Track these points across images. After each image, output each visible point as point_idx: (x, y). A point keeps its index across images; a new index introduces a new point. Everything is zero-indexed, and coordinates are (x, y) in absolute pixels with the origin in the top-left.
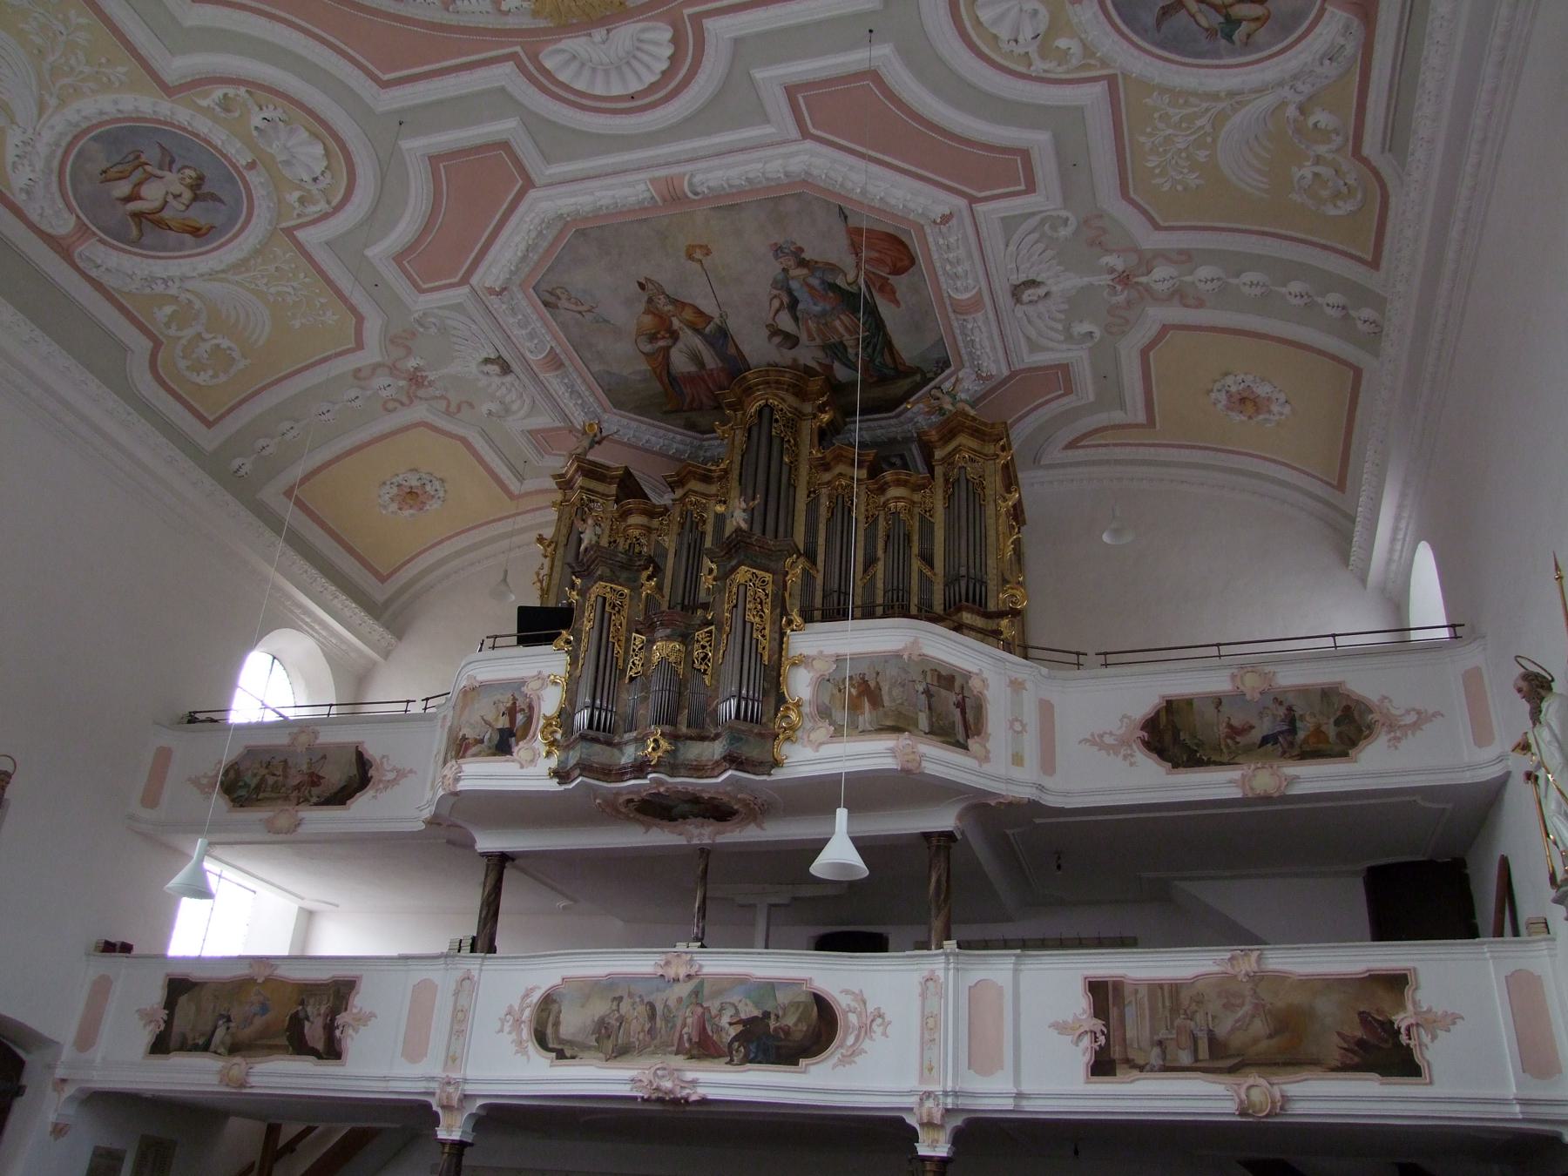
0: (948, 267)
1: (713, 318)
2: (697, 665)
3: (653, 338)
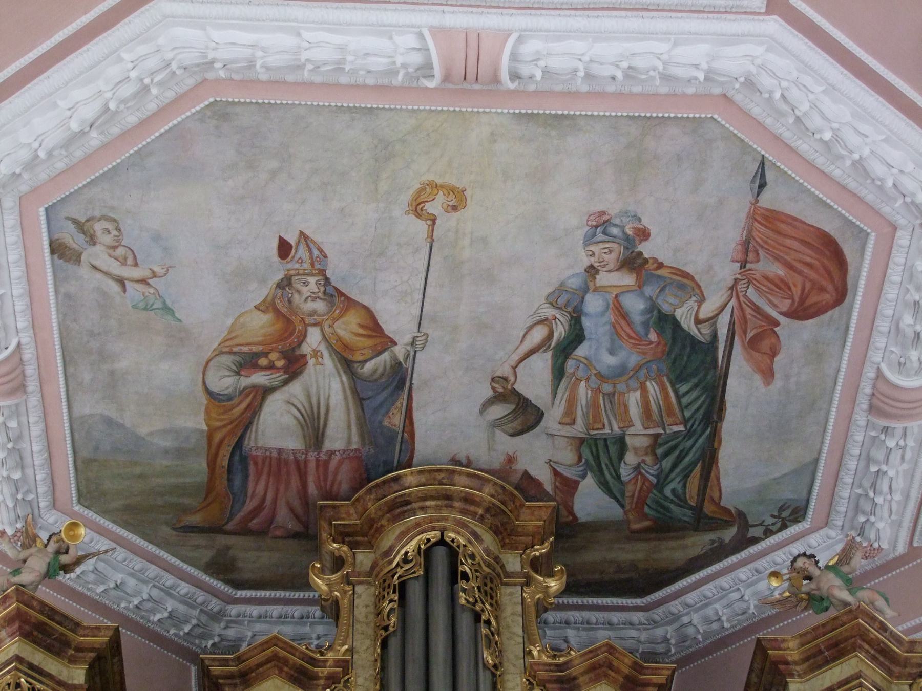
0: (908, 319)
1: (395, 343)
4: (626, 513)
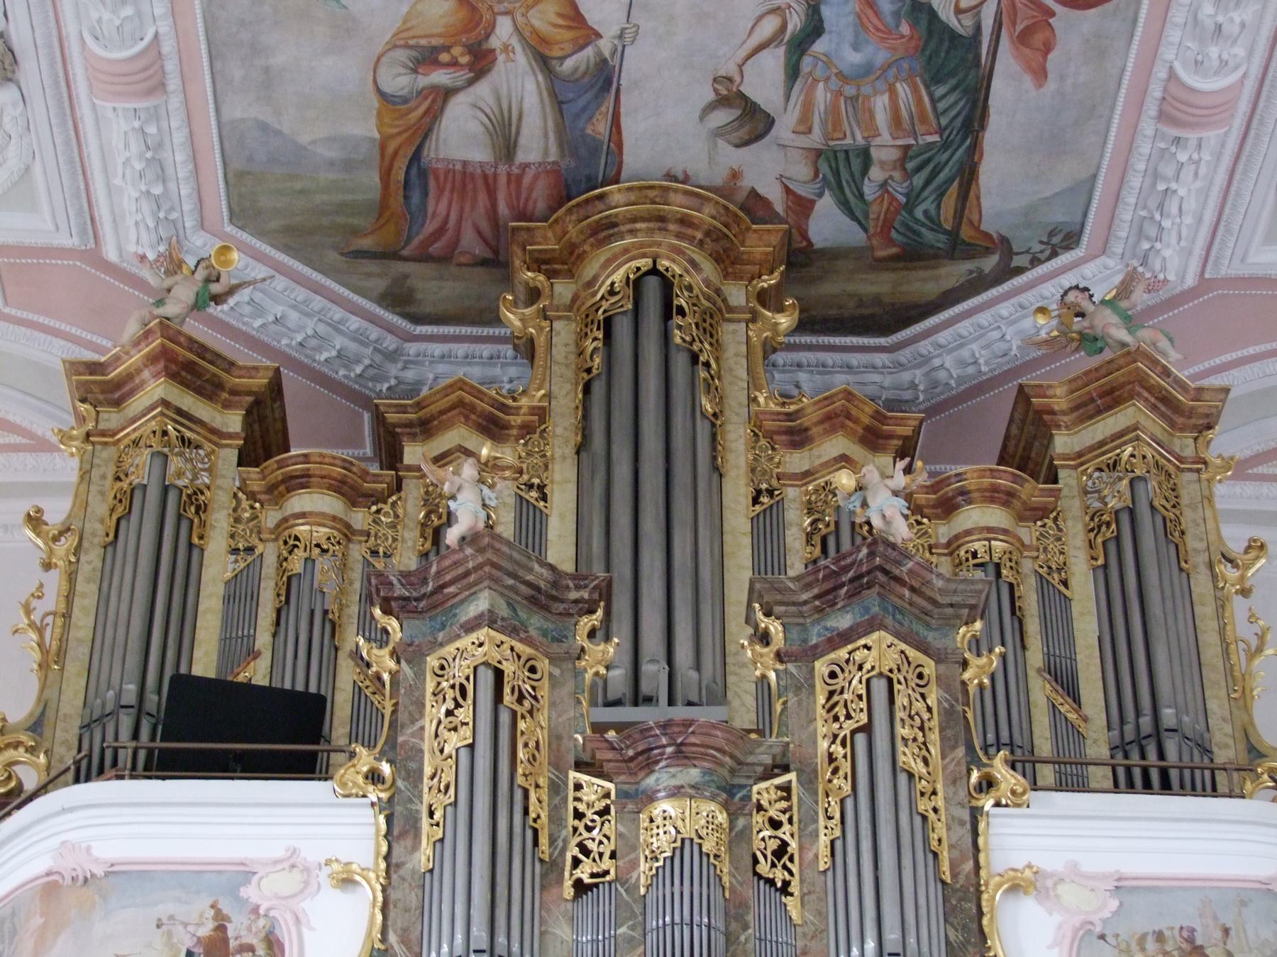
1: (599, 36)
2: (763, 868)
3: (427, 58)
4: (869, 238)
